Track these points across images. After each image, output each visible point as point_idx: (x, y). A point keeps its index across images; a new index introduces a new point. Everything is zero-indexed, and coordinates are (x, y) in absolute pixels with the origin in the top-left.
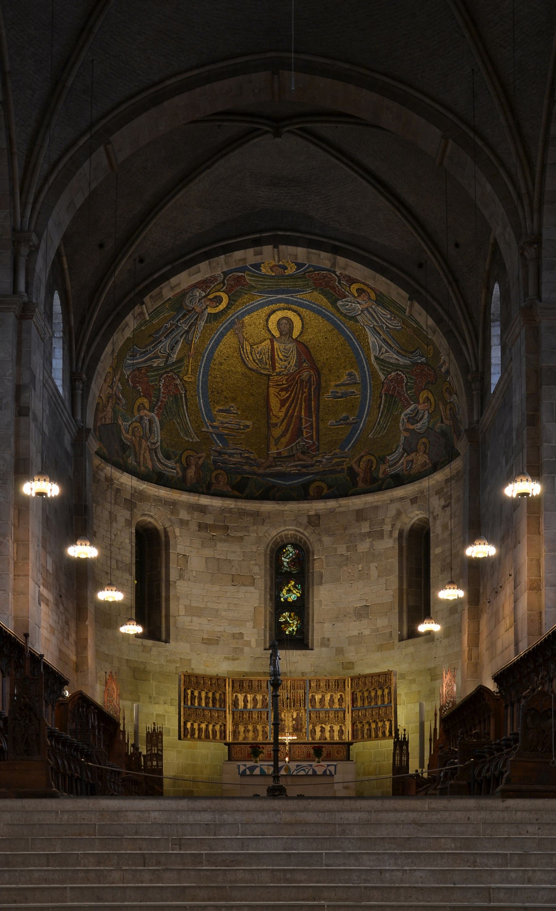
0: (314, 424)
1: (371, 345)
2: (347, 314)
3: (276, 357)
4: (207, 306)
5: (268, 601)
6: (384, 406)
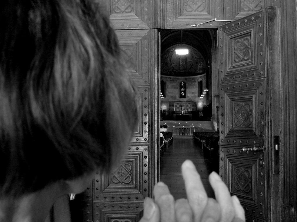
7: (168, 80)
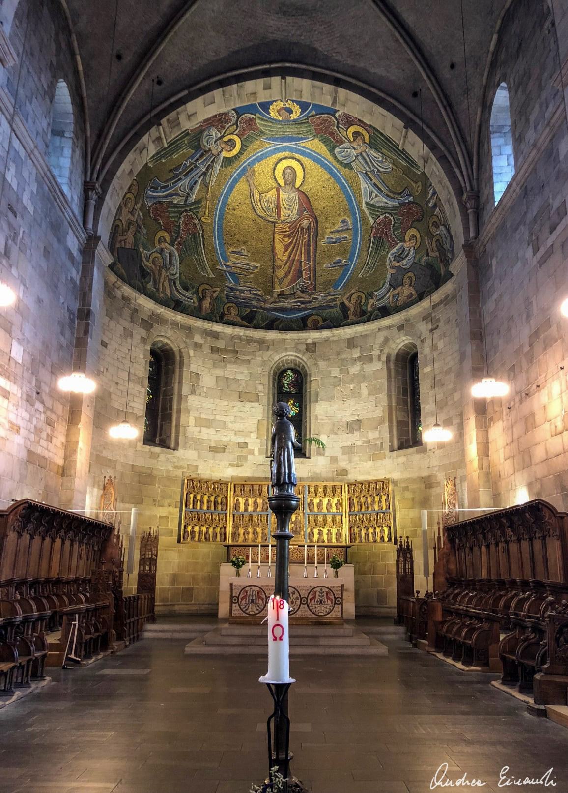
0: (312, 266)
1: (362, 191)
2: (343, 162)
3: (281, 206)
4: (222, 148)
5: (270, 415)
6: (373, 248)
7: (197, 346)
